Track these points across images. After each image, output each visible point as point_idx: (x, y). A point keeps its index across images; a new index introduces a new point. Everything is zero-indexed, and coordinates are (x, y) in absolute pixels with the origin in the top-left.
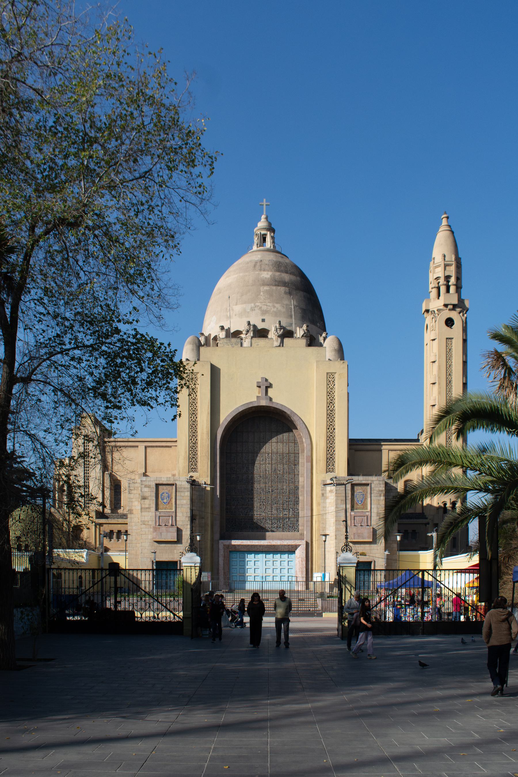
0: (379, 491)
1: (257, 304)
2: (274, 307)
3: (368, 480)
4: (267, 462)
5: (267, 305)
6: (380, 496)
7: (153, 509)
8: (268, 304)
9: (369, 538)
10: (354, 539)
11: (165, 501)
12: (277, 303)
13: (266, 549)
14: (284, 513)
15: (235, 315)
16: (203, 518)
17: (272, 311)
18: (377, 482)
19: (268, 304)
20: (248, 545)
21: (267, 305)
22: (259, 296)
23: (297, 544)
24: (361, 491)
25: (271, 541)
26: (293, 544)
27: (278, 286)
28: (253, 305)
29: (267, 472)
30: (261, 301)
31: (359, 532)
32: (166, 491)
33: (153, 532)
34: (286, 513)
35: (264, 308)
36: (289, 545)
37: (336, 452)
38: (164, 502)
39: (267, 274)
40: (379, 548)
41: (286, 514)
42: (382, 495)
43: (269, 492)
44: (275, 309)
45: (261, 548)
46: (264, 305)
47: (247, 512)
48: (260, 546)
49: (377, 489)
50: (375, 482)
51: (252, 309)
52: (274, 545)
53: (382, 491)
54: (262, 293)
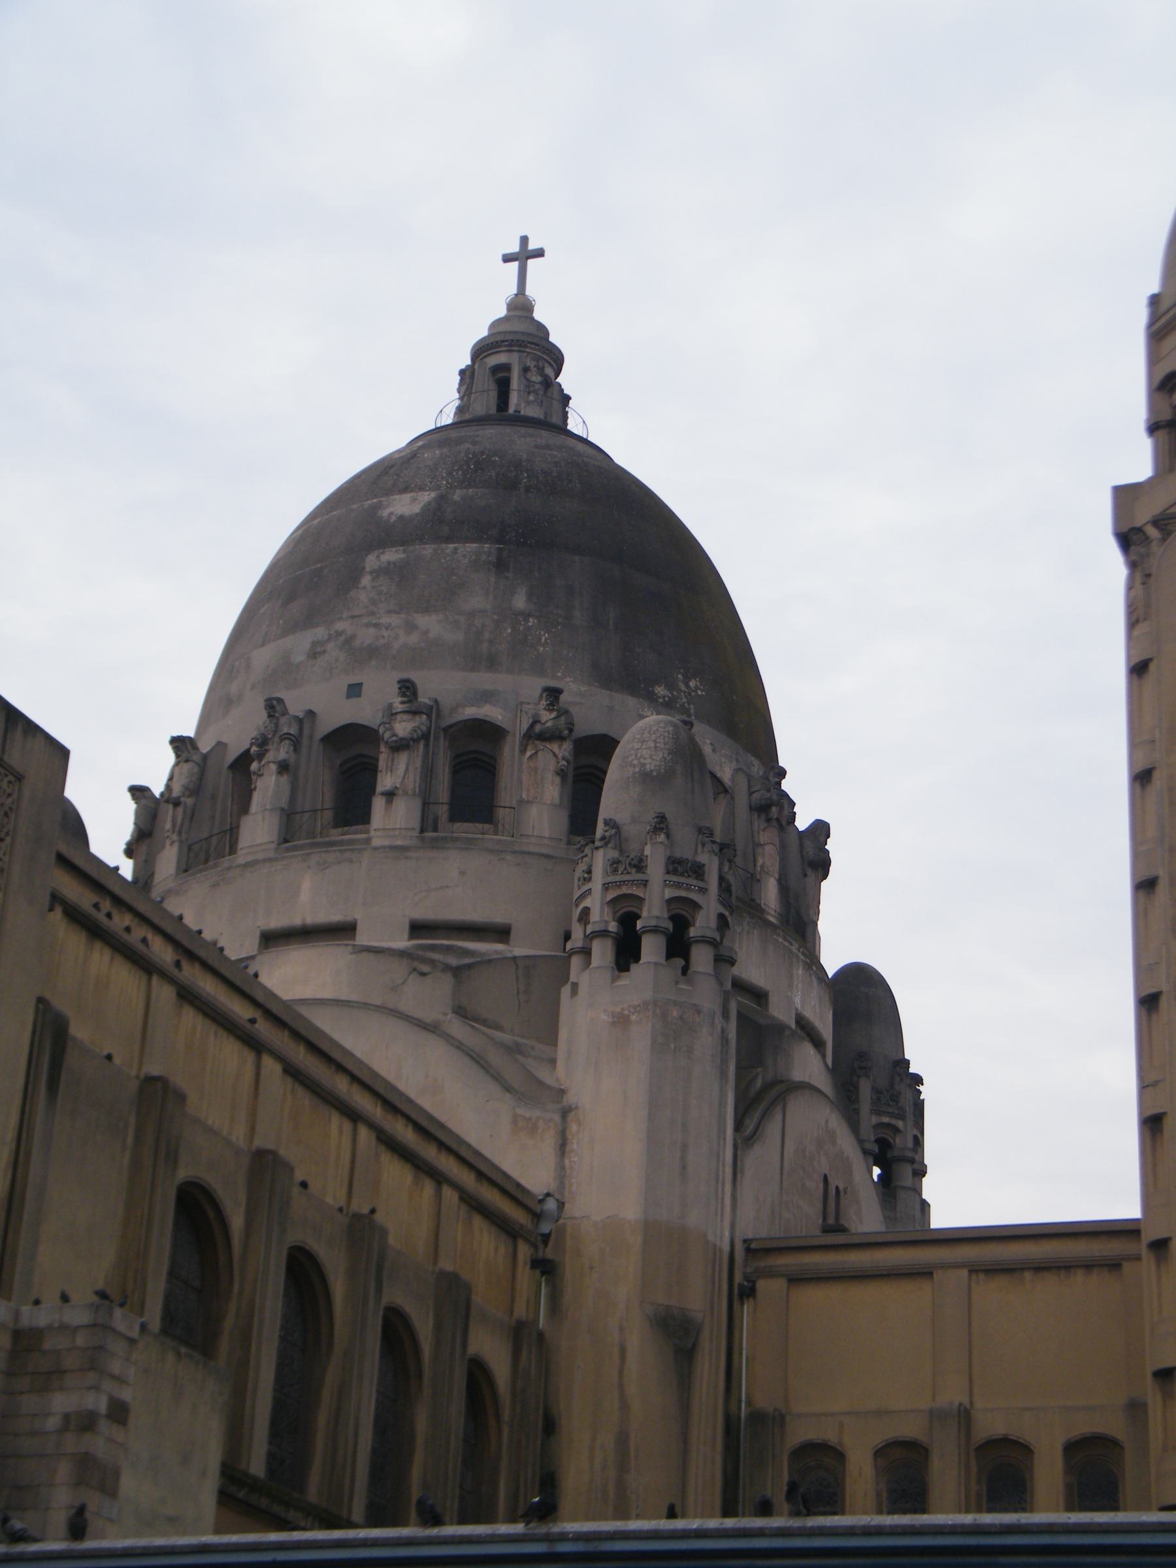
1: (339, 626)
2: (411, 627)
5: (376, 625)
8: (385, 620)
12: (426, 611)
15: (253, 687)
17: (396, 645)
19: (385, 620)
21: (376, 625)
22: (352, 594)
27: (448, 540)
28: (320, 632)
30: (356, 612)
35: (366, 637)
39: (414, 500)
44: (414, 639)
46: (368, 625)
51: (314, 654)
54: (366, 581)
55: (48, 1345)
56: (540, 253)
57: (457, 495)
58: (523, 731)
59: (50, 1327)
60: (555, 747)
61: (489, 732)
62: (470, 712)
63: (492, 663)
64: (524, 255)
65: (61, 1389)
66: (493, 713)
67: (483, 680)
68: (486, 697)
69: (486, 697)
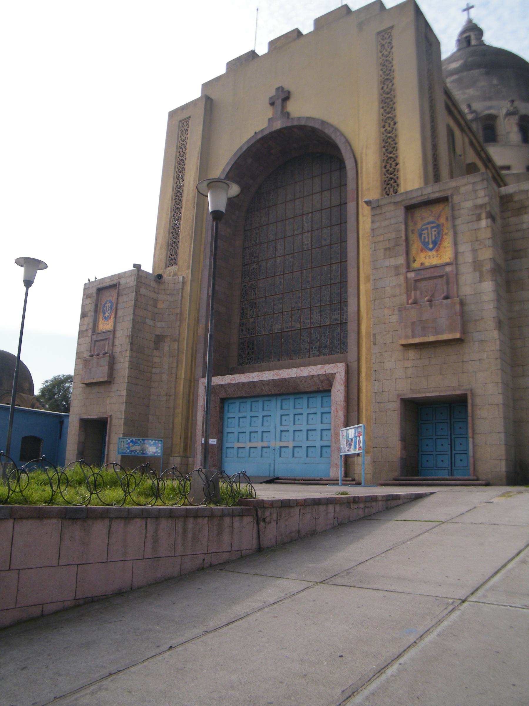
0: (476, 207)
3: (444, 190)
4: (306, 229)
6: (479, 219)
7: (90, 331)
9: (452, 330)
10: (413, 337)
11: (107, 315)
13: (275, 391)
14: (333, 317)
16: (175, 341)
18: (470, 187)
20: (243, 384)
23: (328, 372)
24: (431, 219)
25: (280, 372)
26: (320, 373)
29: (305, 247)
31: (425, 316)
32: (110, 298)
33: (83, 369)
34: (337, 317)
36: (312, 377)
37: (401, 166)
38: (105, 317)
40: (484, 356)
41: (336, 320)
42: (484, 215)
43: (308, 282)
45: (267, 388)
47: (272, 325)
48: (263, 383)
49: (469, 204)
50: (462, 190)
52: (285, 379)
53: (481, 206)
55: (516, 198)
56: (472, 7)
57: (470, 59)
58: (504, 114)
59: (515, 193)
60: (514, 116)
61: (492, 118)
62: (487, 112)
63: (490, 99)
64: (468, 8)
65: (526, 213)
66: (493, 112)
67: (489, 103)
68: (490, 108)
69: (490, 108)
